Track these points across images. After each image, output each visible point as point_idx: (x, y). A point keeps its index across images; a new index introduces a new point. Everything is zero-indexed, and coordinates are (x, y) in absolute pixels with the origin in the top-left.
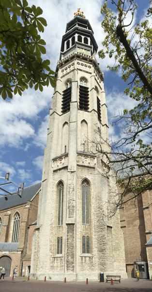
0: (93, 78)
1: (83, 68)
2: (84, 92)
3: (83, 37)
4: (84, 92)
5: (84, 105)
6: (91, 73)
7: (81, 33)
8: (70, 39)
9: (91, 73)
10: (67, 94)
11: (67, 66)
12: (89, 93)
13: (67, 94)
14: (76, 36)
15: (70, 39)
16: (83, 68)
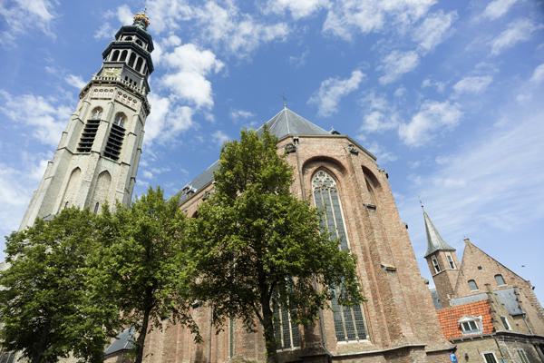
0: (136, 118)
1: (126, 101)
2: (116, 136)
3: (138, 56)
4: (116, 136)
5: (112, 150)
6: (135, 111)
7: (136, 50)
8: (121, 51)
9: (135, 111)
10: (92, 127)
11: (104, 88)
12: (125, 137)
13: (92, 127)
14: (130, 51)
15: (121, 51)
16: (126, 101)
